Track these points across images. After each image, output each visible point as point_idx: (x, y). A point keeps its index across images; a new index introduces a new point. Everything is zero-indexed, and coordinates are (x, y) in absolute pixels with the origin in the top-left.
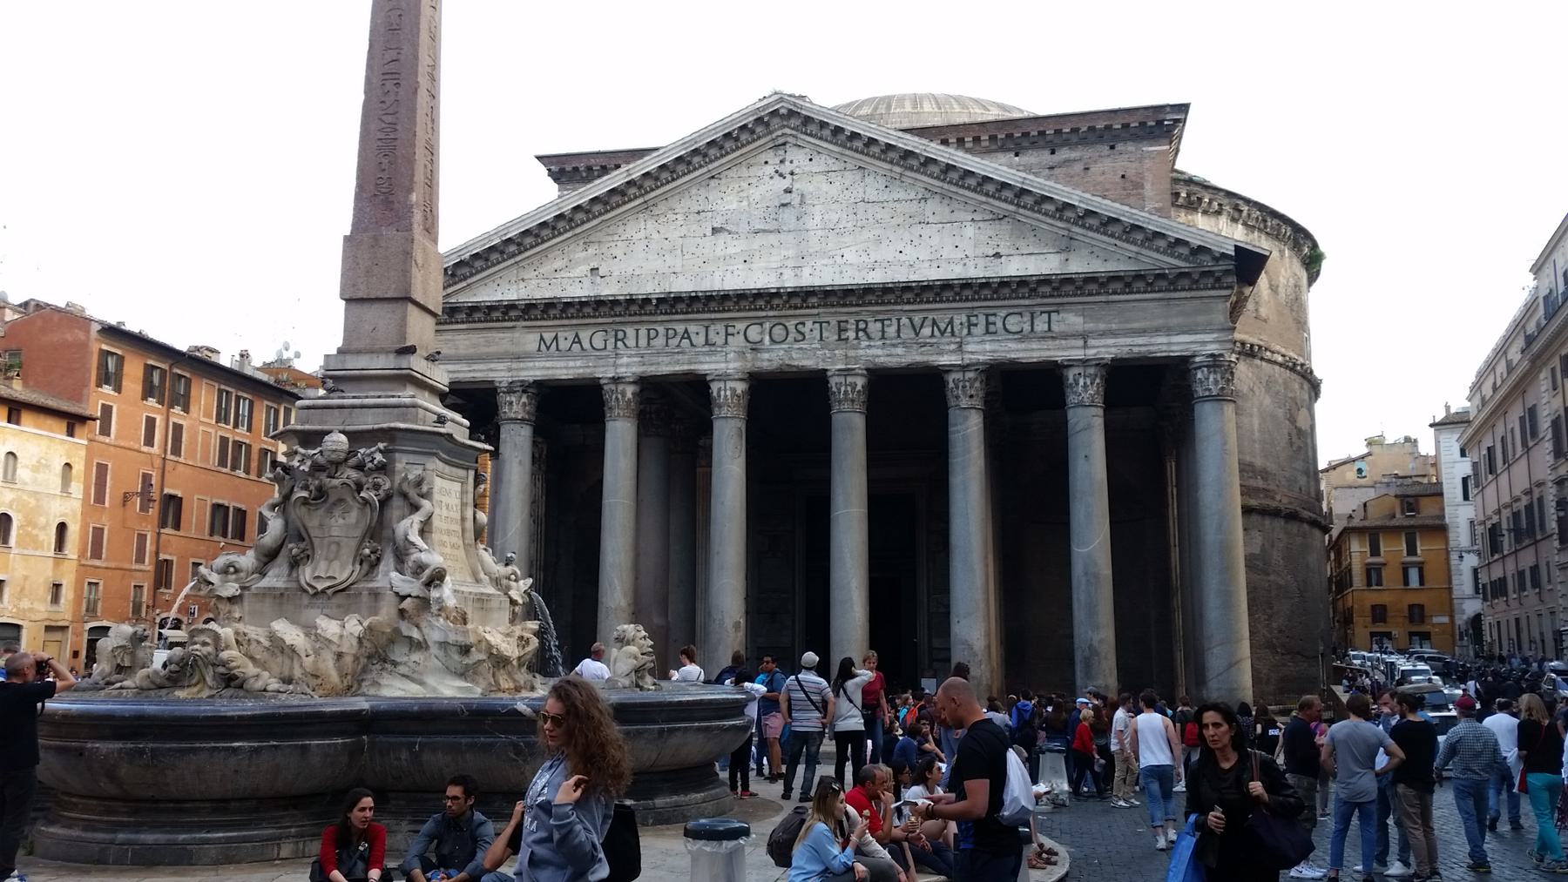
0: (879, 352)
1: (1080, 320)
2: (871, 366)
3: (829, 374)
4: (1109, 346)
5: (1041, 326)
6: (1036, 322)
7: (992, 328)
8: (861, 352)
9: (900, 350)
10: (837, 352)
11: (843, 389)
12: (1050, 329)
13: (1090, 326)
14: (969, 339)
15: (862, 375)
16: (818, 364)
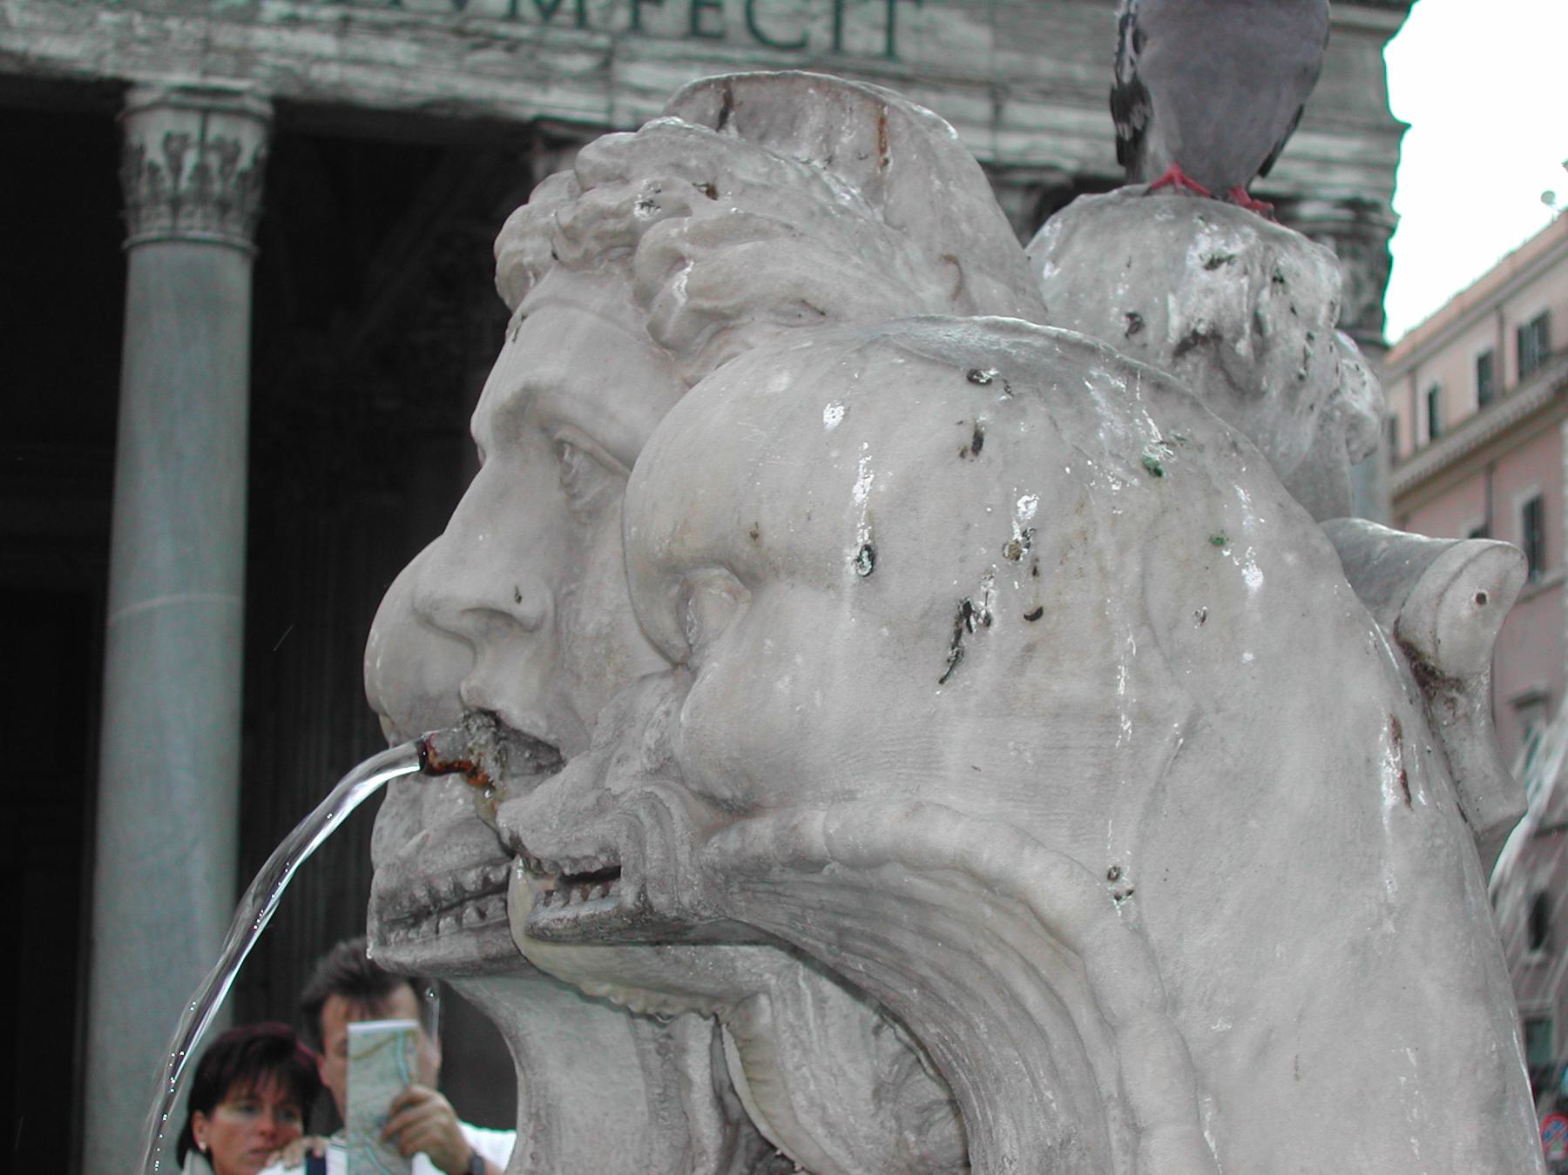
0: (327, 44)
1: (980, 35)
2: (293, 91)
3: (139, 98)
4: (1061, 132)
5: (863, 37)
6: (851, 21)
7: (709, 20)
8: (262, 37)
9: (399, 49)
10: (173, 24)
11: (190, 159)
12: (890, 52)
13: (1009, 60)
14: (635, 44)
15: (258, 118)
16: (100, 57)
